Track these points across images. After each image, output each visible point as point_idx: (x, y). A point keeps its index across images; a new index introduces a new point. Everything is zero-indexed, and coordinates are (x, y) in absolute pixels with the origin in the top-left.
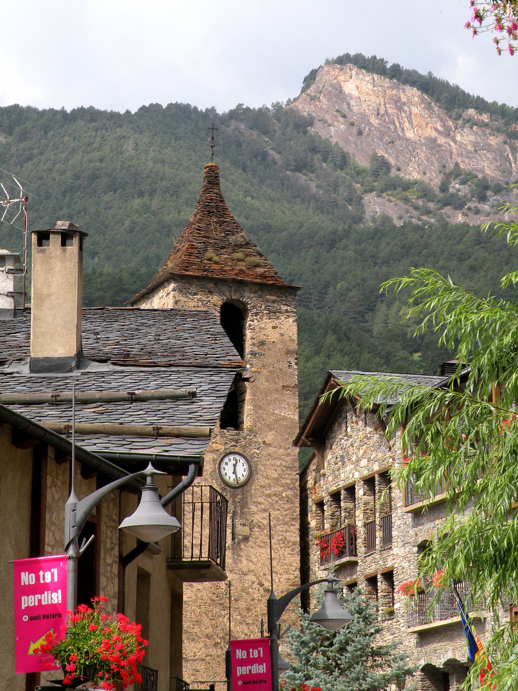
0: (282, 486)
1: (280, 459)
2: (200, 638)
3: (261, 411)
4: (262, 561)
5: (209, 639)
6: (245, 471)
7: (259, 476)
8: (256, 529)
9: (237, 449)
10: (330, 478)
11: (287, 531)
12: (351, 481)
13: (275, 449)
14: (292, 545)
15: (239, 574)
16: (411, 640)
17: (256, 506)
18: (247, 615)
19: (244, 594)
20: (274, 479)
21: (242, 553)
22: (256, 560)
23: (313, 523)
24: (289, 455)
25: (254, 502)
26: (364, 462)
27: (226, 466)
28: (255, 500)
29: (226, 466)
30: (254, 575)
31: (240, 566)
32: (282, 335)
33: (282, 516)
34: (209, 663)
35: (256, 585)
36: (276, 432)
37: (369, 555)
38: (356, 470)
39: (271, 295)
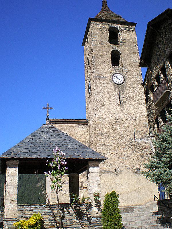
9: (118, 72)
18: (128, 129)
19: (126, 121)
24: (138, 74)
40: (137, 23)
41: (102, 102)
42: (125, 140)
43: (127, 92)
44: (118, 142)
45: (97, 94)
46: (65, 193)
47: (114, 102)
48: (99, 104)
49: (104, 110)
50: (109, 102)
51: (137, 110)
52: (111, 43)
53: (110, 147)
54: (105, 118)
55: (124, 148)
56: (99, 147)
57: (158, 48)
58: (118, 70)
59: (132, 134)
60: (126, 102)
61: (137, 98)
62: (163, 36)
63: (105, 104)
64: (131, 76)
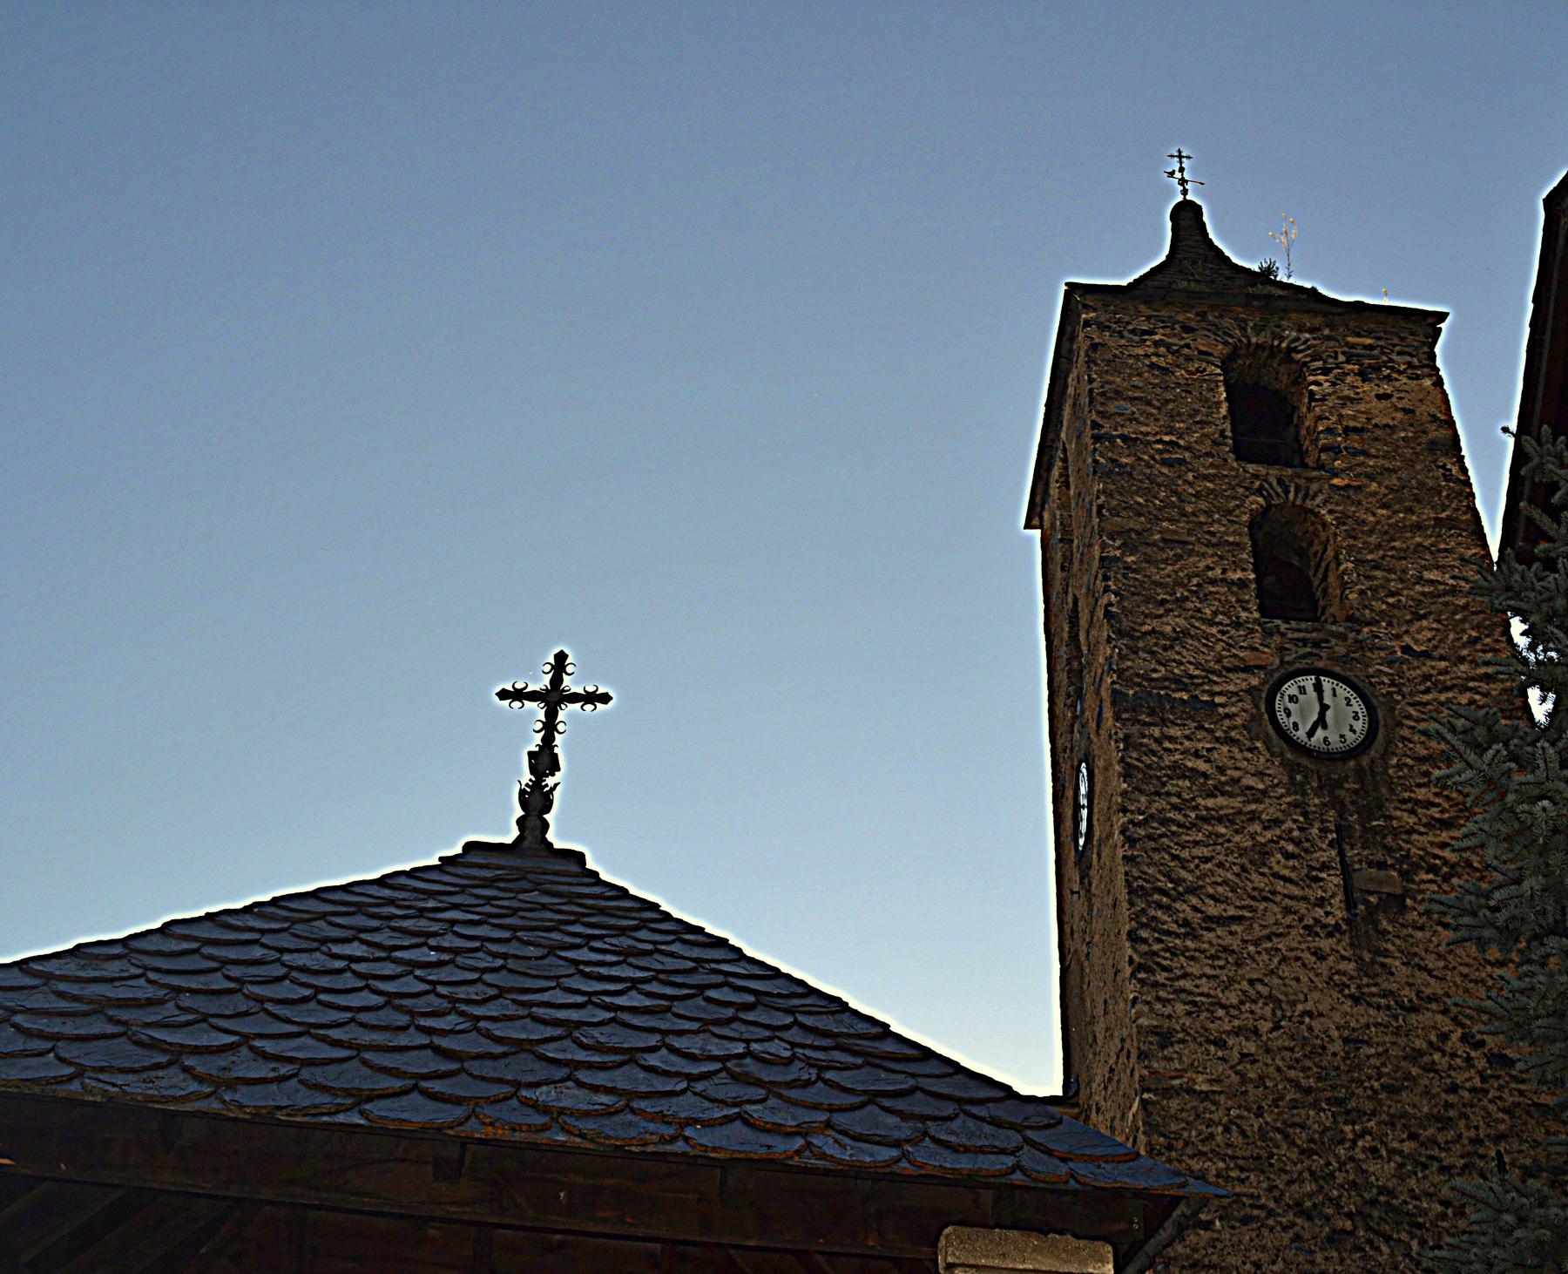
1: (1471, 689)
2: (1271, 1213)
3: (1377, 573)
4: (1465, 970)
5: (1310, 1218)
6: (1356, 717)
15: (1388, 1007)
17: (1412, 812)
18: (1440, 1139)
22: (1441, 964)
25: (1404, 801)
28: (1406, 795)
40: (1442, 316)
42: (1415, 1245)
47: (1302, 907)
49: (1208, 971)
50: (1248, 902)
54: (1220, 1043)
60: (1408, 901)
63: (1220, 921)
64: (1427, 691)
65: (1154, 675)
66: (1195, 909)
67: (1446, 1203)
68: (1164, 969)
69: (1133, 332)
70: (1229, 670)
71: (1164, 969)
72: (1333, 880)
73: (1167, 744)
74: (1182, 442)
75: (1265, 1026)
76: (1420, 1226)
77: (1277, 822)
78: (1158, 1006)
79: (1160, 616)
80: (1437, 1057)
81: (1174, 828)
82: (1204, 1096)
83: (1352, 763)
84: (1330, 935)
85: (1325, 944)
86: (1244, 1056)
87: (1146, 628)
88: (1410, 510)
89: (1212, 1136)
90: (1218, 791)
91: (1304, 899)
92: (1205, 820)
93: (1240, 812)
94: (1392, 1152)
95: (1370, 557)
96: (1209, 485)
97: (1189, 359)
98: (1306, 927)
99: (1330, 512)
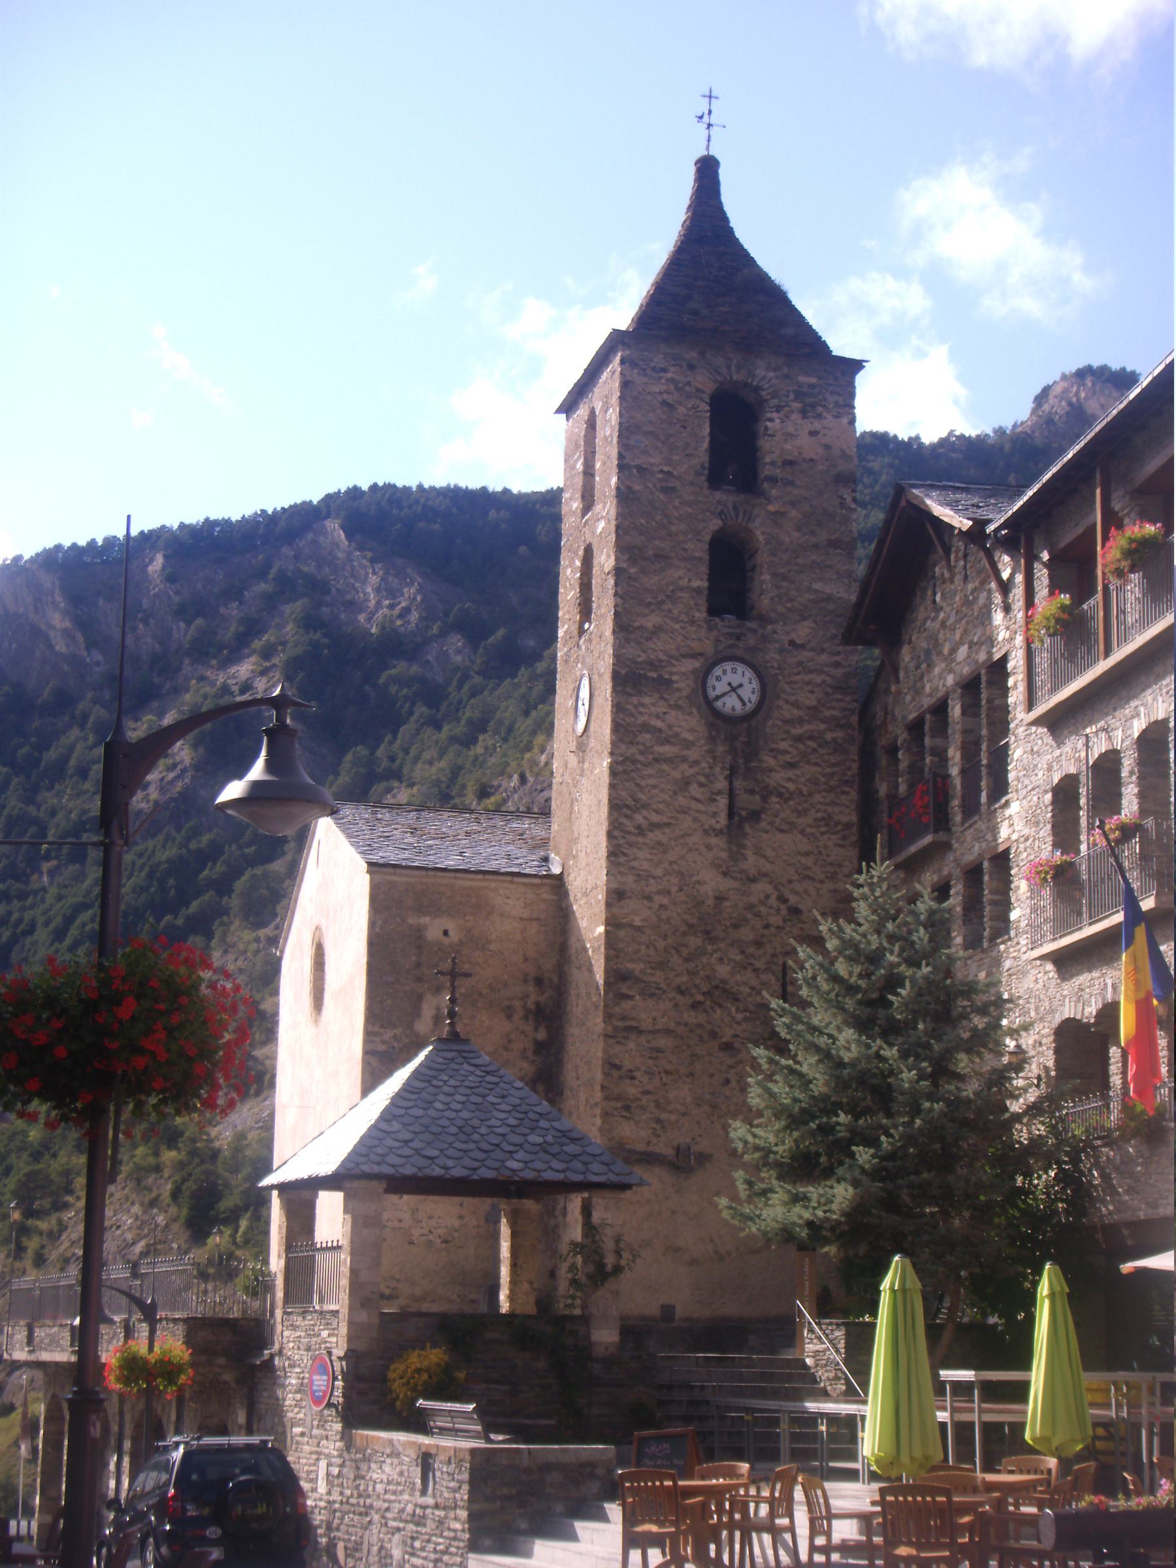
0: (824, 722)
1: (821, 672)
2: (664, 992)
3: (784, 584)
6: (753, 693)
7: (780, 703)
8: (774, 799)
10: (908, 698)
11: (833, 803)
12: (941, 694)
13: (810, 654)
14: (843, 830)
16: (1039, 976)
17: (775, 757)
19: (749, 916)
20: (809, 708)
21: (747, 842)
23: (883, 789)
24: (837, 665)
25: (771, 750)
26: (963, 652)
27: (717, 684)
28: (773, 746)
29: (717, 684)
30: (771, 882)
31: (744, 865)
32: (827, 447)
33: (824, 775)
34: (682, 1038)
35: (773, 901)
36: (815, 622)
37: (970, 827)
38: (951, 671)
39: (807, 374)
41: (645, 812)
42: (733, 1009)
43: (770, 761)
44: (701, 1018)
45: (620, 768)
46: (425, 1231)
47: (703, 818)
48: (625, 821)
49: (649, 856)
51: (808, 861)
52: (715, 478)
53: (663, 1042)
54: (649, 898)
55: (727, 1047)
56: (611, 1041)
57: (934, 602)
58: (738, 638)
59: (773, 981)
60: (763, 816)
61: (817, 798)
62: (955, 567)
64: (799, 674)
65: (639, 659)
66: (645, 818)
67: (753, 988)
68: (624, 854)
69: (654, 369)
70: (684, 656)
71: (624, 854)
72: (723, 802)
73: (641, 709)
74: (675, 473)
75: (674, 889)
76: (737, 1000)
77: (697, 763)
78: (619, 877)
79: (645, 616)
80: (762, 908)
81: (639, 766)
82: (639, 929)
83: (746, 725)
84: (717, 835)
85: (713, 841)
86: (662, 906)
87: (636, 624)
88: (813, 533)
89: (639, 950)
90: (667, 741)
91: (706, 813)
92: (657, 760)
93: (677, 756)
94: (730, 960)
95: (782, 571)
96: (689, 510)
97: (689, 396)
98: (705, 831)
99: (763, 533)
